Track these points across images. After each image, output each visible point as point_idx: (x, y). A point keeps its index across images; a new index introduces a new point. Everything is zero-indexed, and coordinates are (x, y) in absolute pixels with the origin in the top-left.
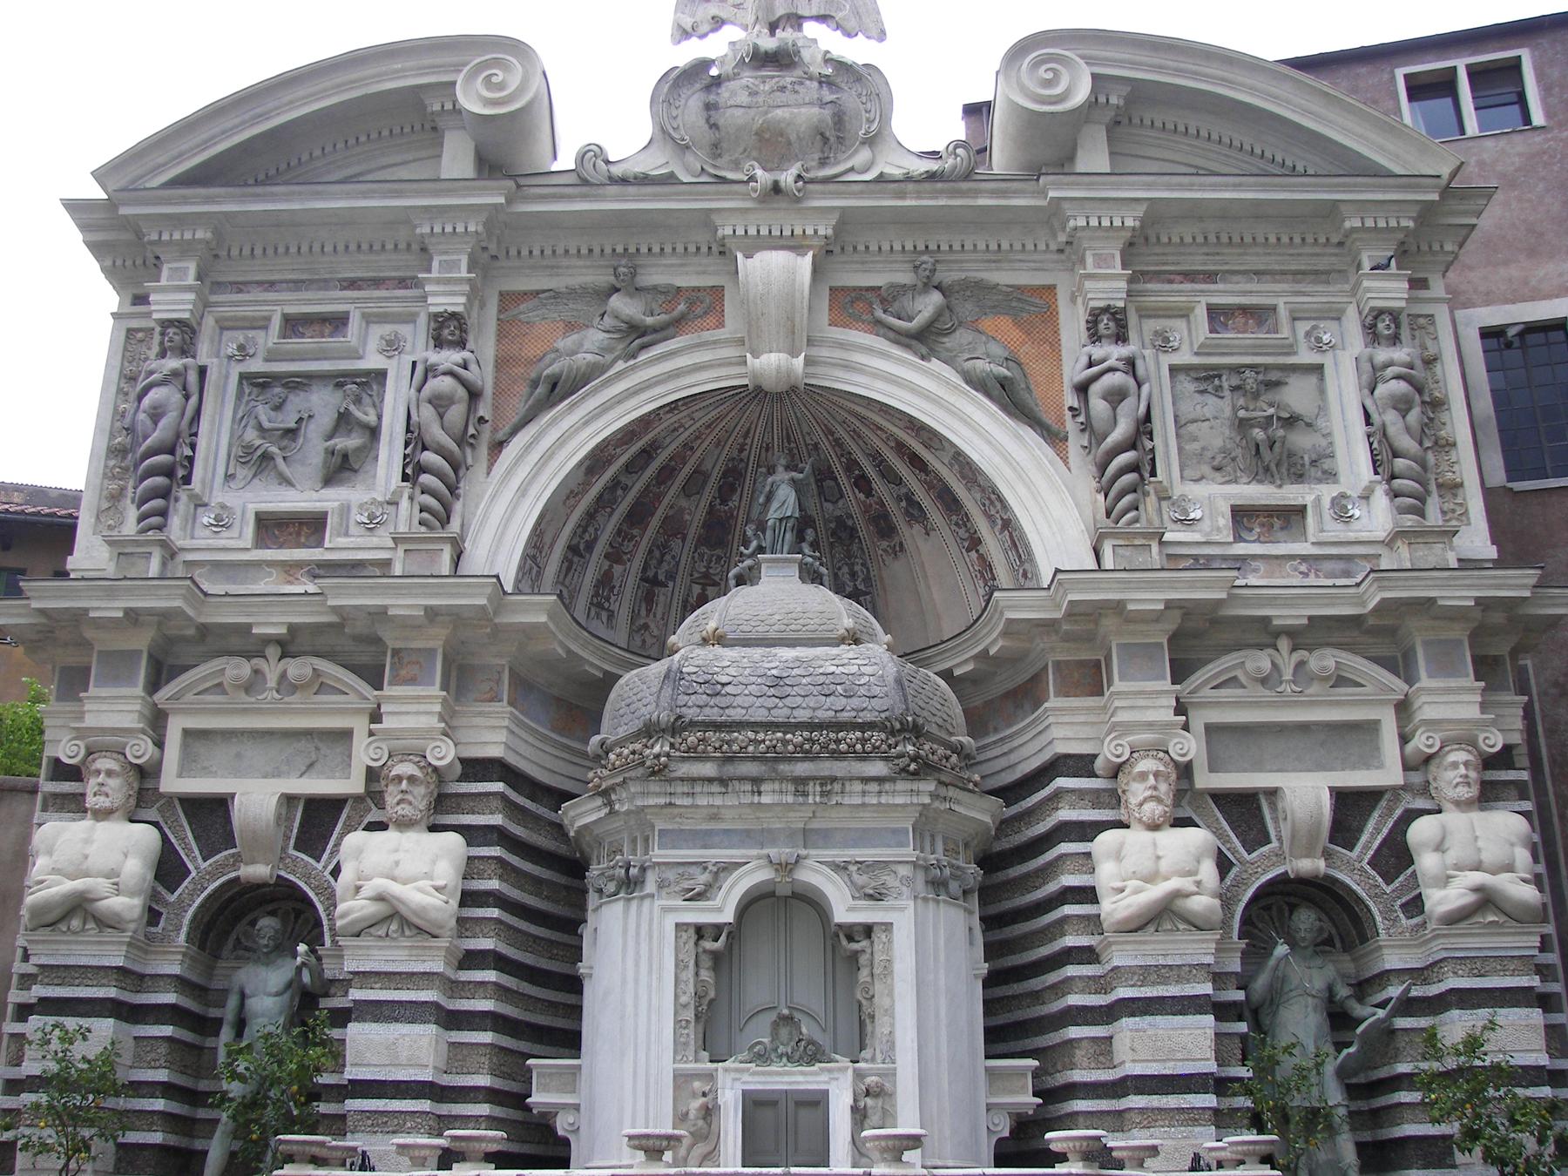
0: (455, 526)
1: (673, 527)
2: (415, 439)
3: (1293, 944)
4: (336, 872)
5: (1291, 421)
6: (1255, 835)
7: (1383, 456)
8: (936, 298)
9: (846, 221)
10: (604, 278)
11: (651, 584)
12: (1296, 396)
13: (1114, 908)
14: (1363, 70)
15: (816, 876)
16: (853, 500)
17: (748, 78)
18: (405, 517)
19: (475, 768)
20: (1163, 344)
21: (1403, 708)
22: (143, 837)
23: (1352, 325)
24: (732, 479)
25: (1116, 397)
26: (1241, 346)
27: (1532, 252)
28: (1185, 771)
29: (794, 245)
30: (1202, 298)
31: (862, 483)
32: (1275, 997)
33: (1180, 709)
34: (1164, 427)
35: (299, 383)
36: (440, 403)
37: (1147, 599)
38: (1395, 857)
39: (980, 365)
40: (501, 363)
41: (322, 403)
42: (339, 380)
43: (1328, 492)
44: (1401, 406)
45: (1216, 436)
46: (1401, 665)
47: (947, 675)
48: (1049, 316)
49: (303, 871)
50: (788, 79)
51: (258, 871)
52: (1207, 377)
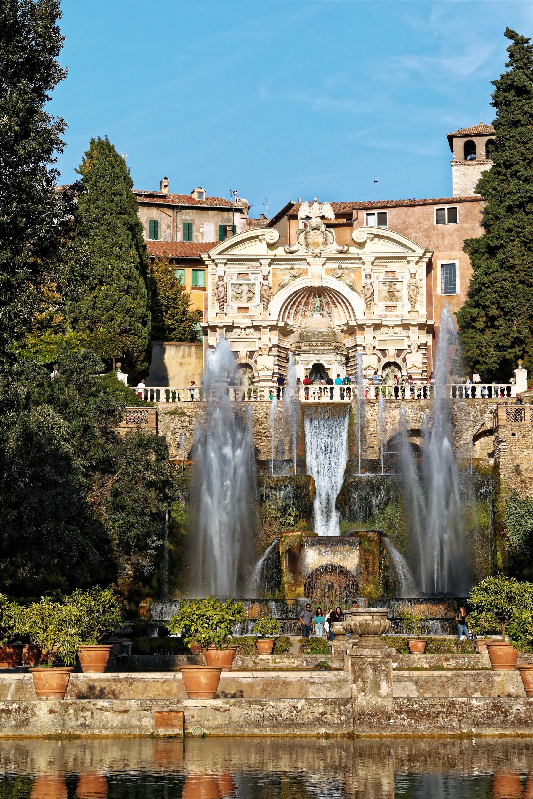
0: (268, 311)
2: (262, 296)
4: (256, 362)
5: (397, 291)
6: (385, 356)
7: (410, 298)
8: (341, 271)
9: (328, 259)
10: (289, 267)
12: (398, 287)
14: (428, 207)
16: (329, 299)
17: (312, 232)
18: (261, 308)
19: (274, 346)
20: (378, 277)
21: (408, 337)
23: (409, 275)
25: (368, 289)
26: (390, 279)
27: (452, 249)
30: (384, 269)
31: (330, 297)
33: (374, 337)
35: (241, 285)
36: (265, 291)
37: (369, 323)
38: (404, 360)
39: (348, 283)
40: (273, 281)
41: (245, 288)
42: (248, 284)
44: (413, 290)
45: (385, 294)
48: (360, 273)
49: (251, 362)
50: (319, 232)
51: (244, 361)
52: (385, 283)
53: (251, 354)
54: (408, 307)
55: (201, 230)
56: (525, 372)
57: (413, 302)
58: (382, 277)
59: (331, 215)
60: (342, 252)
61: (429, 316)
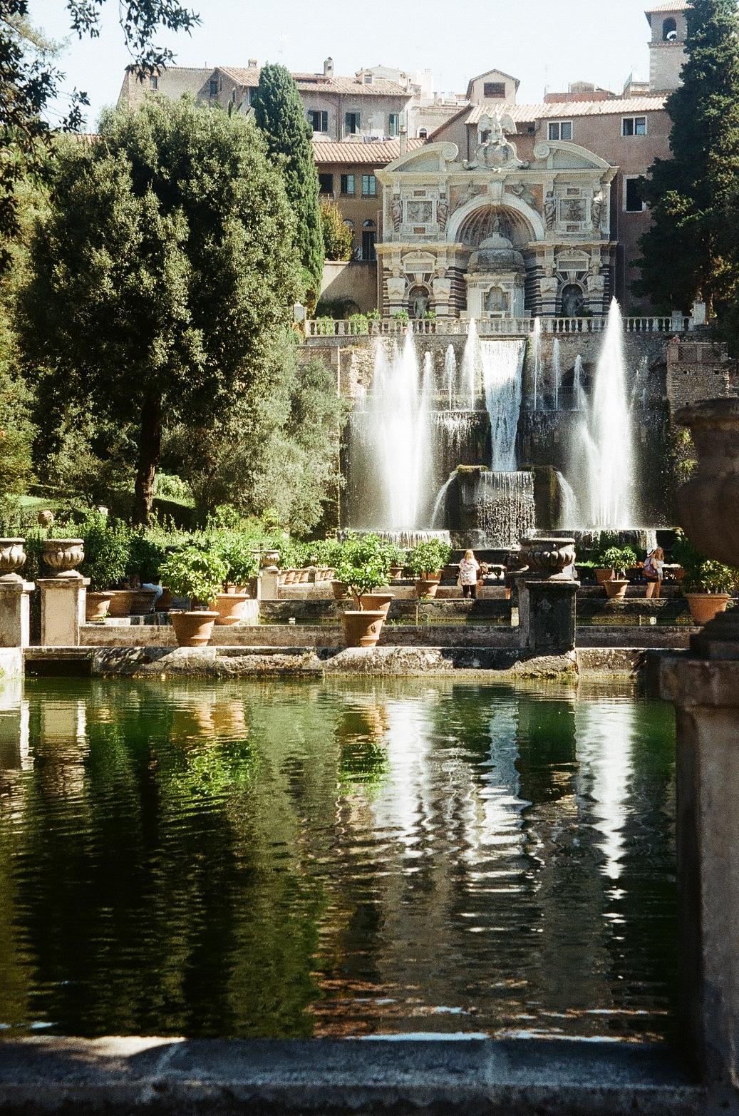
1: (478, 222)
3: (571, 294)
4: (432, 284)
11: (474, 231)
13: (542, 289)
15: (500, 285)
22: (403, 281)
24: (488, 215)
26: (573, 197)
28: (555, 269)
29: (497, 181)
30: (565, 187)
32: (568, 301)
33: (555, 259)
34: (558, 212)
38: (585, 282)
41: (422, 207)
42: (425, 202)
43: (583, 222)
45: (566, 212)
46: (589, 253)
47: (521, 251)
51: (419, 285)
53: (427, 277)
54: (591, 227)
55: (370, 121)
56: (703, 306)
57: (597, 221)
58: (565, 196)
59: (514, 130)
60: (522, 168)
61: (613, 238)
